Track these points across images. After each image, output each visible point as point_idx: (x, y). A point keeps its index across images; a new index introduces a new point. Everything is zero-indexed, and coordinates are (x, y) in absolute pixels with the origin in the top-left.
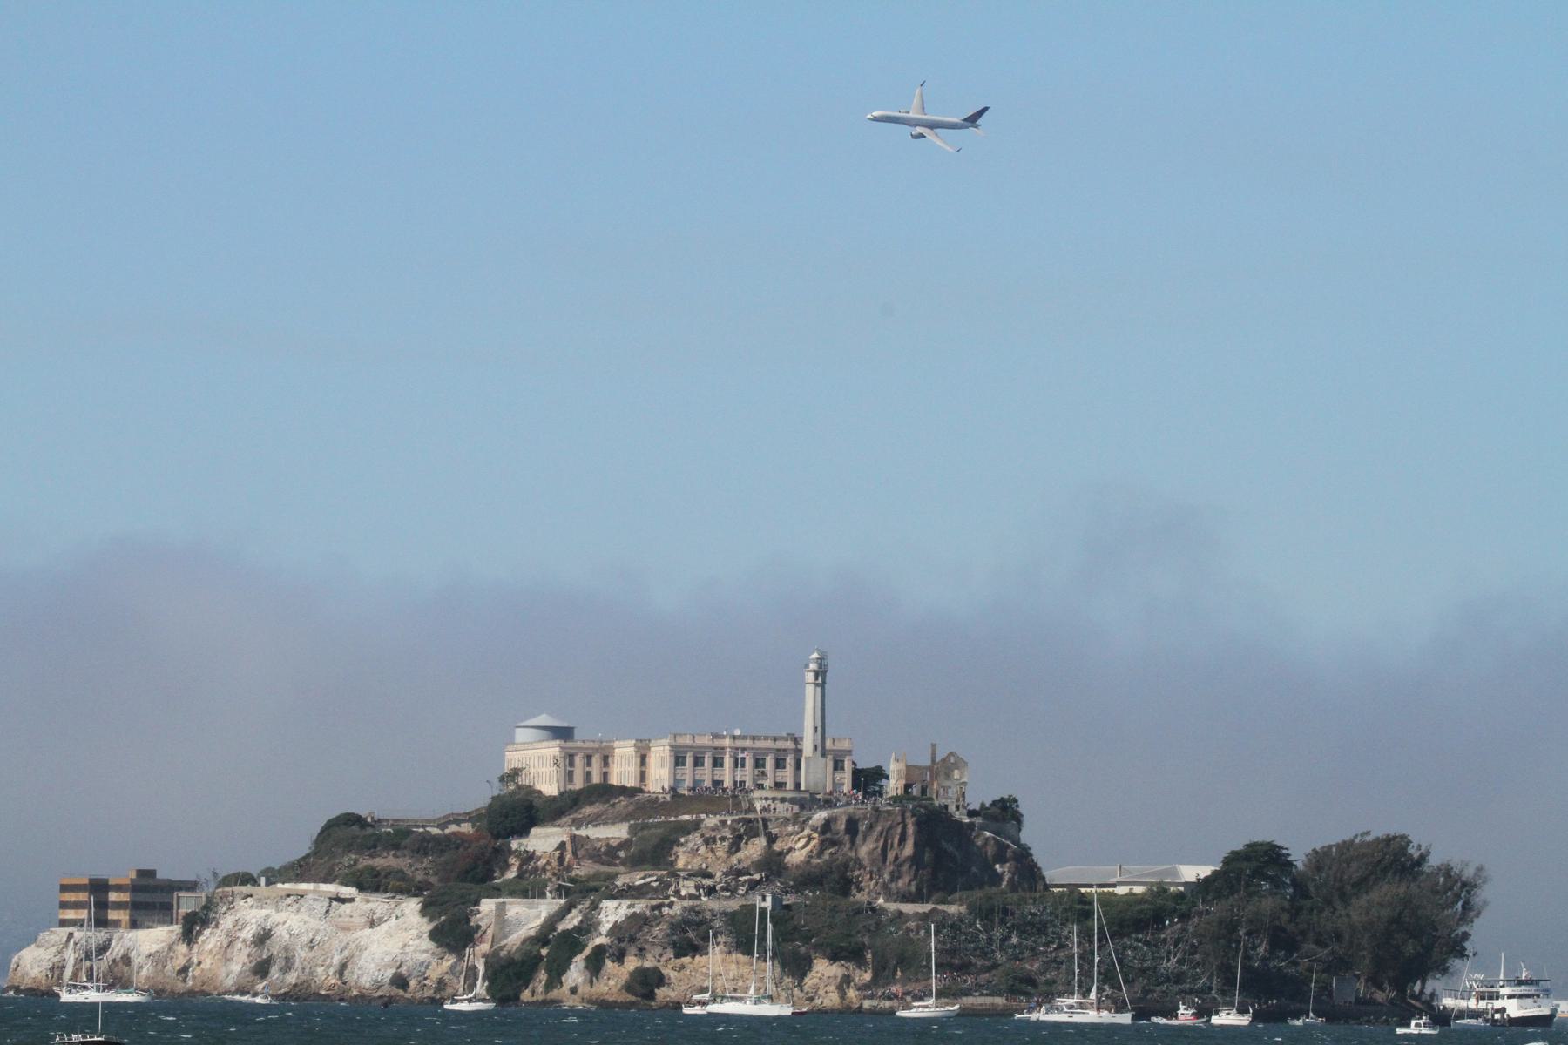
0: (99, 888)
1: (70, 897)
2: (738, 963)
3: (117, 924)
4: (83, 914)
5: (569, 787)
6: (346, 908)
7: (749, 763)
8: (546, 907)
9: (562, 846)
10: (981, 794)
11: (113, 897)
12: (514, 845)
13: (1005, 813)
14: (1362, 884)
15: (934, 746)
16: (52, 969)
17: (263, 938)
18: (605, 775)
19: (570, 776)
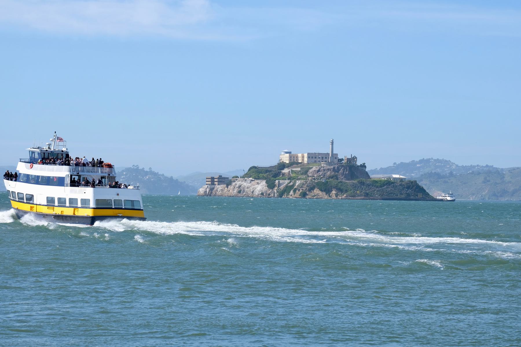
0: (213, 179)
1: (207, 180)
3: (216, 184)
4: (210, 183)
5: (291, 161)
6: (253, 182)
7: (321, 158)
8: (287, 182)
9: (290, 171)
10: (359, 163)
11: (215, 180)
13: (364, 166)
15: (351, 155)
16: (205, 192)
17: (240, 187)
19: (291, 159)
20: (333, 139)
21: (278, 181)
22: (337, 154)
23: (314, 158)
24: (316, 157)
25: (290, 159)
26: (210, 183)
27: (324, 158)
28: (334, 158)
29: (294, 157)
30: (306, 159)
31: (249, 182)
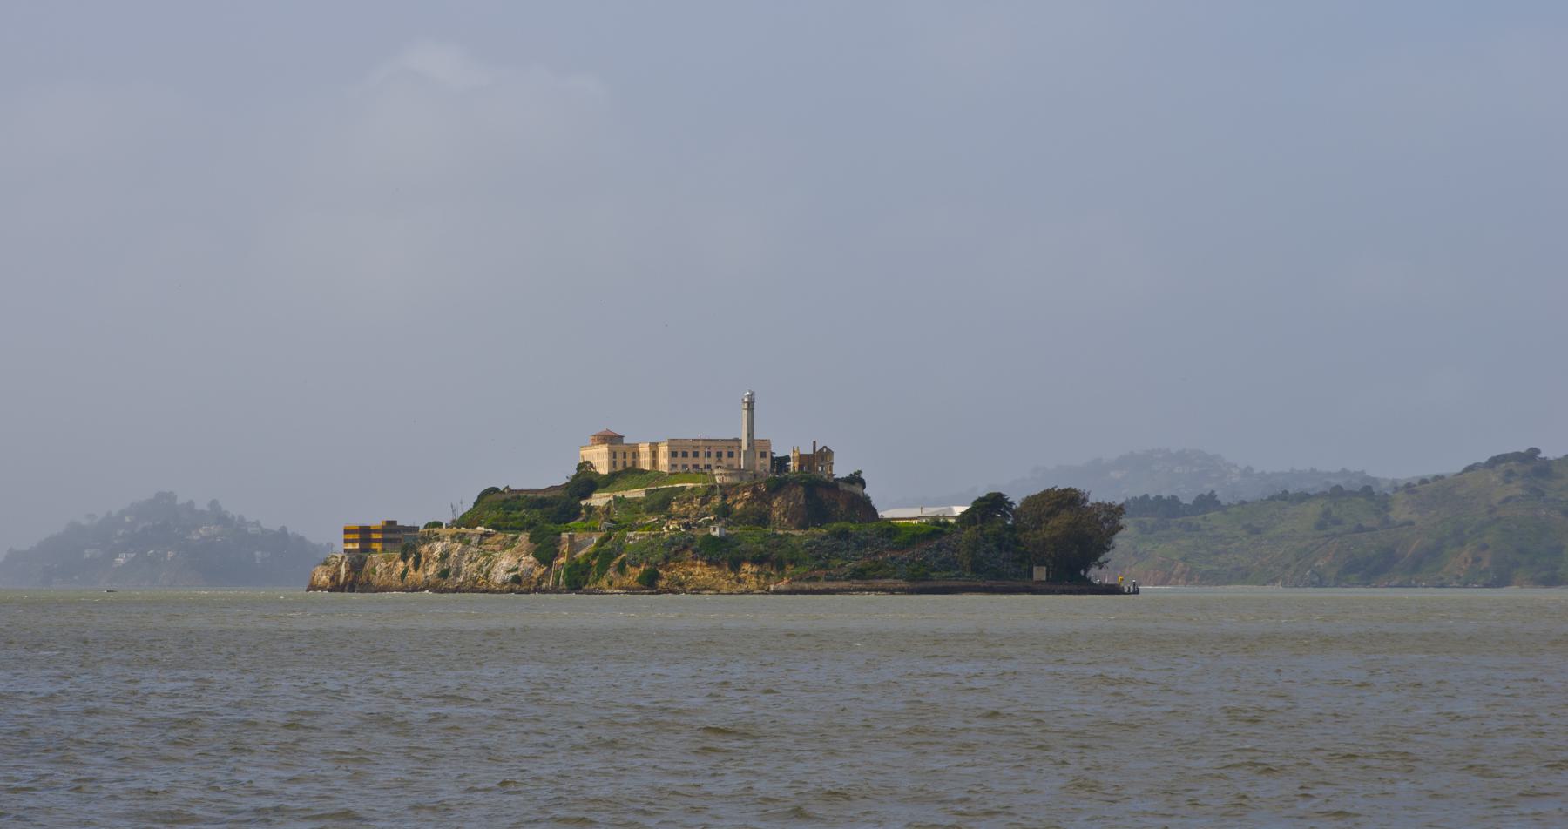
1: (351, 537)
2: (701, 566)
3: (375, 551)
4: (357, 546)
5: (613, 470)
7: (713, 454)
9: (610, 501)
10: (841, 470)
11: (375, 536)
12: (583, 503)
13: (856, 479)
14: (1052, 514)
15: (814, 442)
17: (444, 556)
18: (634, 463)
19: (615, 462)
21: (570, 535)
23: (690, 454)
24: (697, 452)
26: (357, 546)
27: (725, 454)
28: (758, 455)
29: (625, 453)
30: (664, 462)
31: (475, 540)
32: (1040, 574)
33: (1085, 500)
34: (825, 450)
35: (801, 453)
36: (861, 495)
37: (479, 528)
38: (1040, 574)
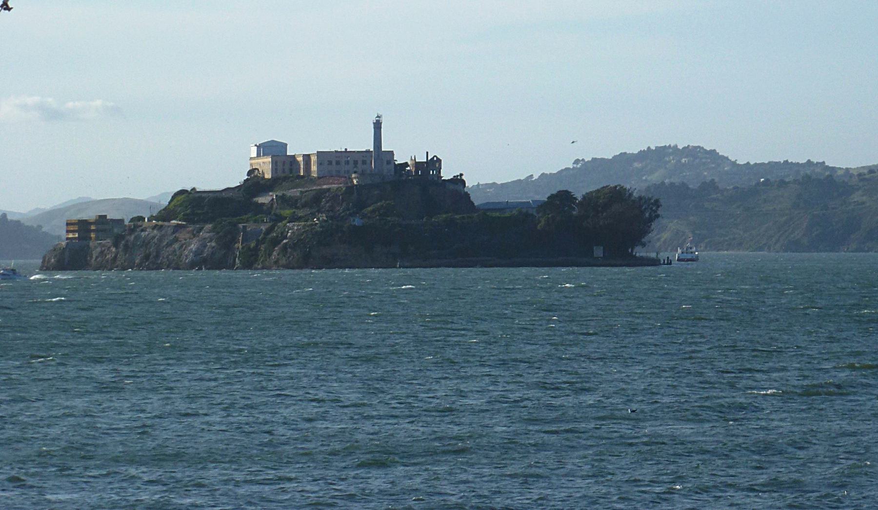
7: (351, 163)
10: (447, 174)
13: (458, 181)
15: (427, 153)
19: (276, 169)
20: (380, 114)
22: (391, 153)
23: (334, 163)
25: (274, 170)
26: (77, 236)
27: (360, 162)
28: (385, 162)
30: (314, 168)
32: (598, 252)
33: (631, 195)
34: (435, 159)
35: (417, 161)
36: (463, 192)
37: (173, 222)
38: (598, 252)
